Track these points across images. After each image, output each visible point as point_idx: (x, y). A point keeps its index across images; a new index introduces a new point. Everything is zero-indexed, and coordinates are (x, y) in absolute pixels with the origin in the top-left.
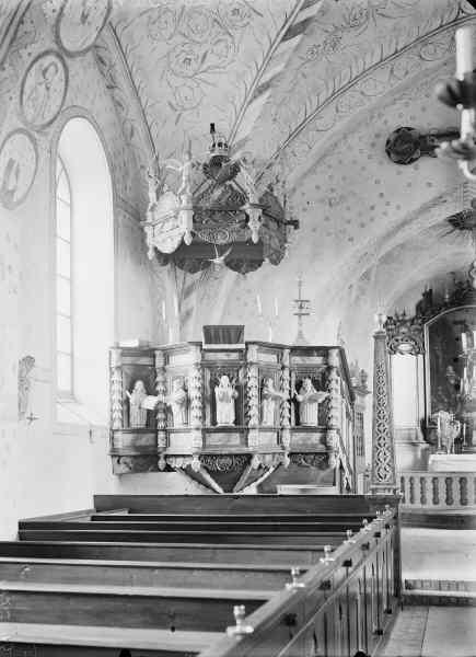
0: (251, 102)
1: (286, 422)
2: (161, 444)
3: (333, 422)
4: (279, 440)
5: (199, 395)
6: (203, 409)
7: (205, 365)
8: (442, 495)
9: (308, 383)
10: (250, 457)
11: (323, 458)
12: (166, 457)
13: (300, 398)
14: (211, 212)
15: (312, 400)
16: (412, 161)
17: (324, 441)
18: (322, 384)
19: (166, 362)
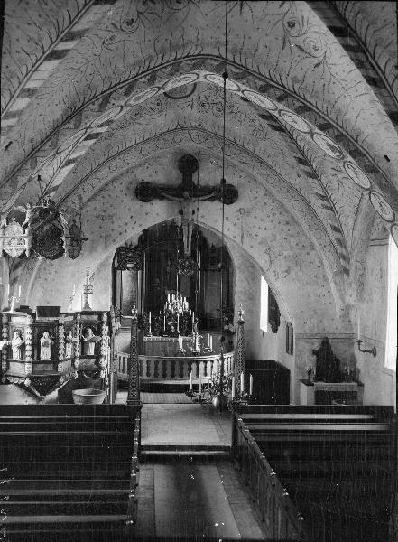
0: (63, 167)
1: (77, 354)
2: (4, 368)
3: (103, 353)
4: (73, 364)
5: (31, 343)
6: (33, 351)
7: (34, 326)
8: (152, 371)
9: (90, 330)
10: (59, 377)
11: (97, 376)
12: (7, 376)
13: (86, 340)
14: (42, 239)
15: (91, 341)
16: (150, 200)
17: (97, 363)
18: (98, 332)
19: (9, 320)
